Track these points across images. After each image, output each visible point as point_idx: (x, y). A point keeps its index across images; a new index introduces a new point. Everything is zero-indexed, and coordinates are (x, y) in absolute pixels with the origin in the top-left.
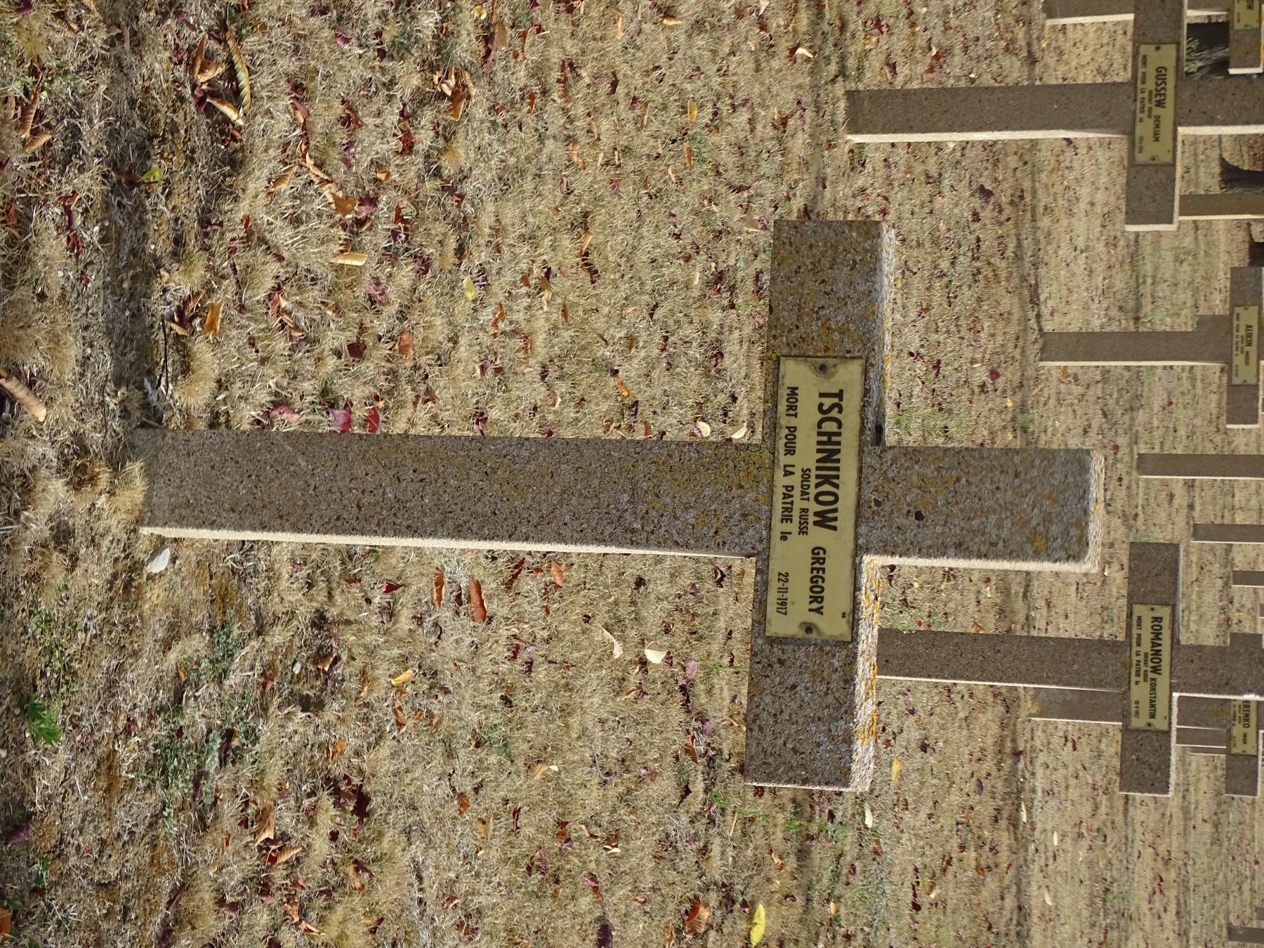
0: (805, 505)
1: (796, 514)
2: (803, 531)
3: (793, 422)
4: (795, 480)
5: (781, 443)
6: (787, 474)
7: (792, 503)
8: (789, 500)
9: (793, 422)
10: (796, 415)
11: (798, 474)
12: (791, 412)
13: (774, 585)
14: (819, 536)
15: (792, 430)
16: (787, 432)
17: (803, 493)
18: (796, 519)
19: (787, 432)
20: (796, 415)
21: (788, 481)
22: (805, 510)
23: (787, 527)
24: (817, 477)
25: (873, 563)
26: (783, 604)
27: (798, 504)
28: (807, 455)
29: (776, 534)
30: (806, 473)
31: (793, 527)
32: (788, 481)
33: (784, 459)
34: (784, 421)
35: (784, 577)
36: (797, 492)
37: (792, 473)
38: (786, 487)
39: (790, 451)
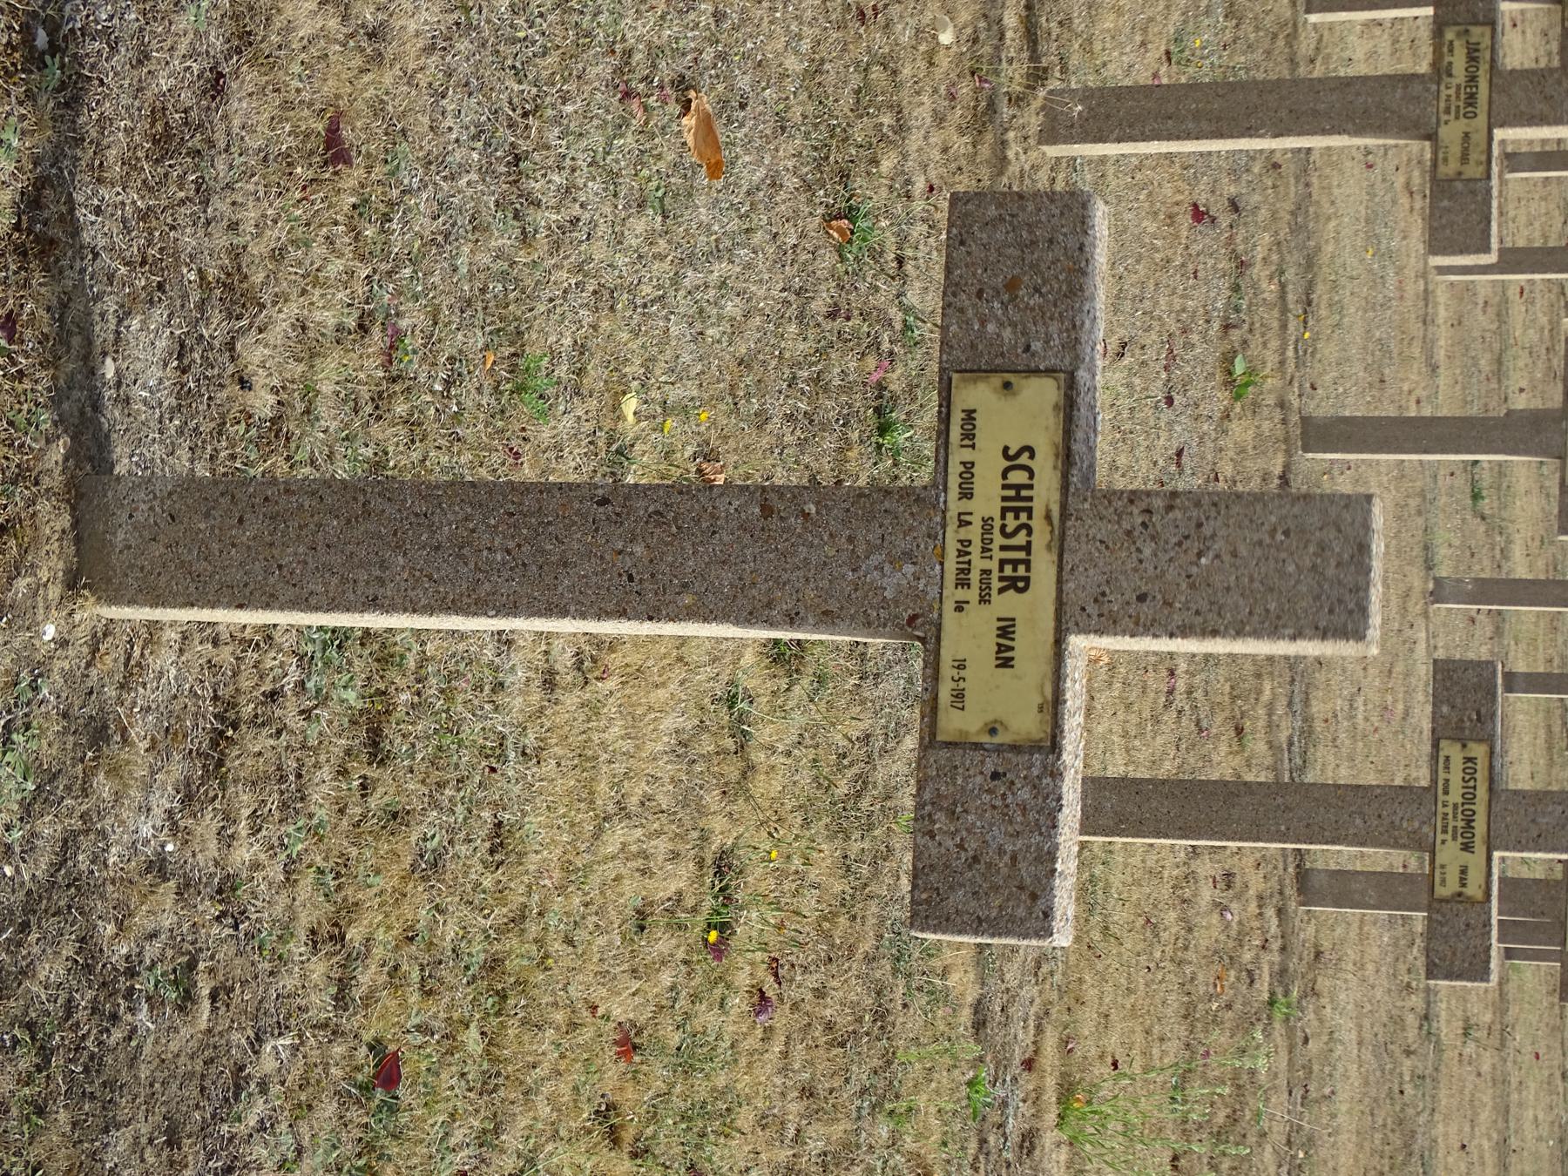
0: (987, 564)
1: (975, 576)
2: (984, 599)
3: (967, 455)
4: (974, 533)
5: (954, 482)
6: (963, 524)
7: (969, 562)
8: (966, 559)
9: (967, 455)
10: (973, 446)
12: (966, 442)
13: (947, 671)
14: (1007, 604)
15: (968, 466)
16: (962, 469)
17: (984, 550)
19: (962, 469)
20: (973, 446)
21: (964, 533)
23: (961, 594)
25: (1078, 643)
26: (959, 696)
27: (978, 563)
28: (988, 500)
29: (949, 606)
30: (987, 522)
31: (972, 594)
32: (964, 533)
33: (955, 506)
34: (958, 456)
35: (961, 665)
36: (975, 549)
37: (969, 523)
38: (961, 541)
39: (967, 494)
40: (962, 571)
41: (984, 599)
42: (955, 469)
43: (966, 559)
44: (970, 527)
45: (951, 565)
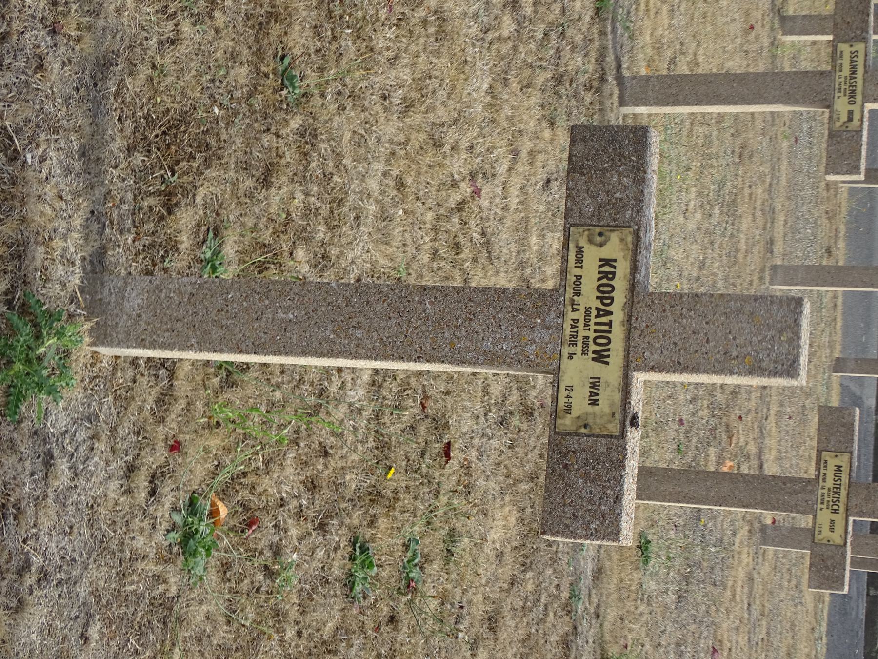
0: (586, 333)
1: (580, 339)
3: (578, 271)
7: (577, 332)
8: (575, 330)
10: (582, 267)
11: (582, 310)
15: (579, 278)
16: (574, 279)
17: (586, 325)
18: (580, 344)
19: (574, 279)
21: (575, 315)
22: (587, 337)
24: (595, 343)
30: (588, 310)
32: (575, 315)
35: (570, 389)
36: (581, 325)
37: (578, 310)
40: (573, 336)
41: (584, 353)
42: (571, 279)
43: (575, 330)
44: (577, 313)
45: (568, 331)
